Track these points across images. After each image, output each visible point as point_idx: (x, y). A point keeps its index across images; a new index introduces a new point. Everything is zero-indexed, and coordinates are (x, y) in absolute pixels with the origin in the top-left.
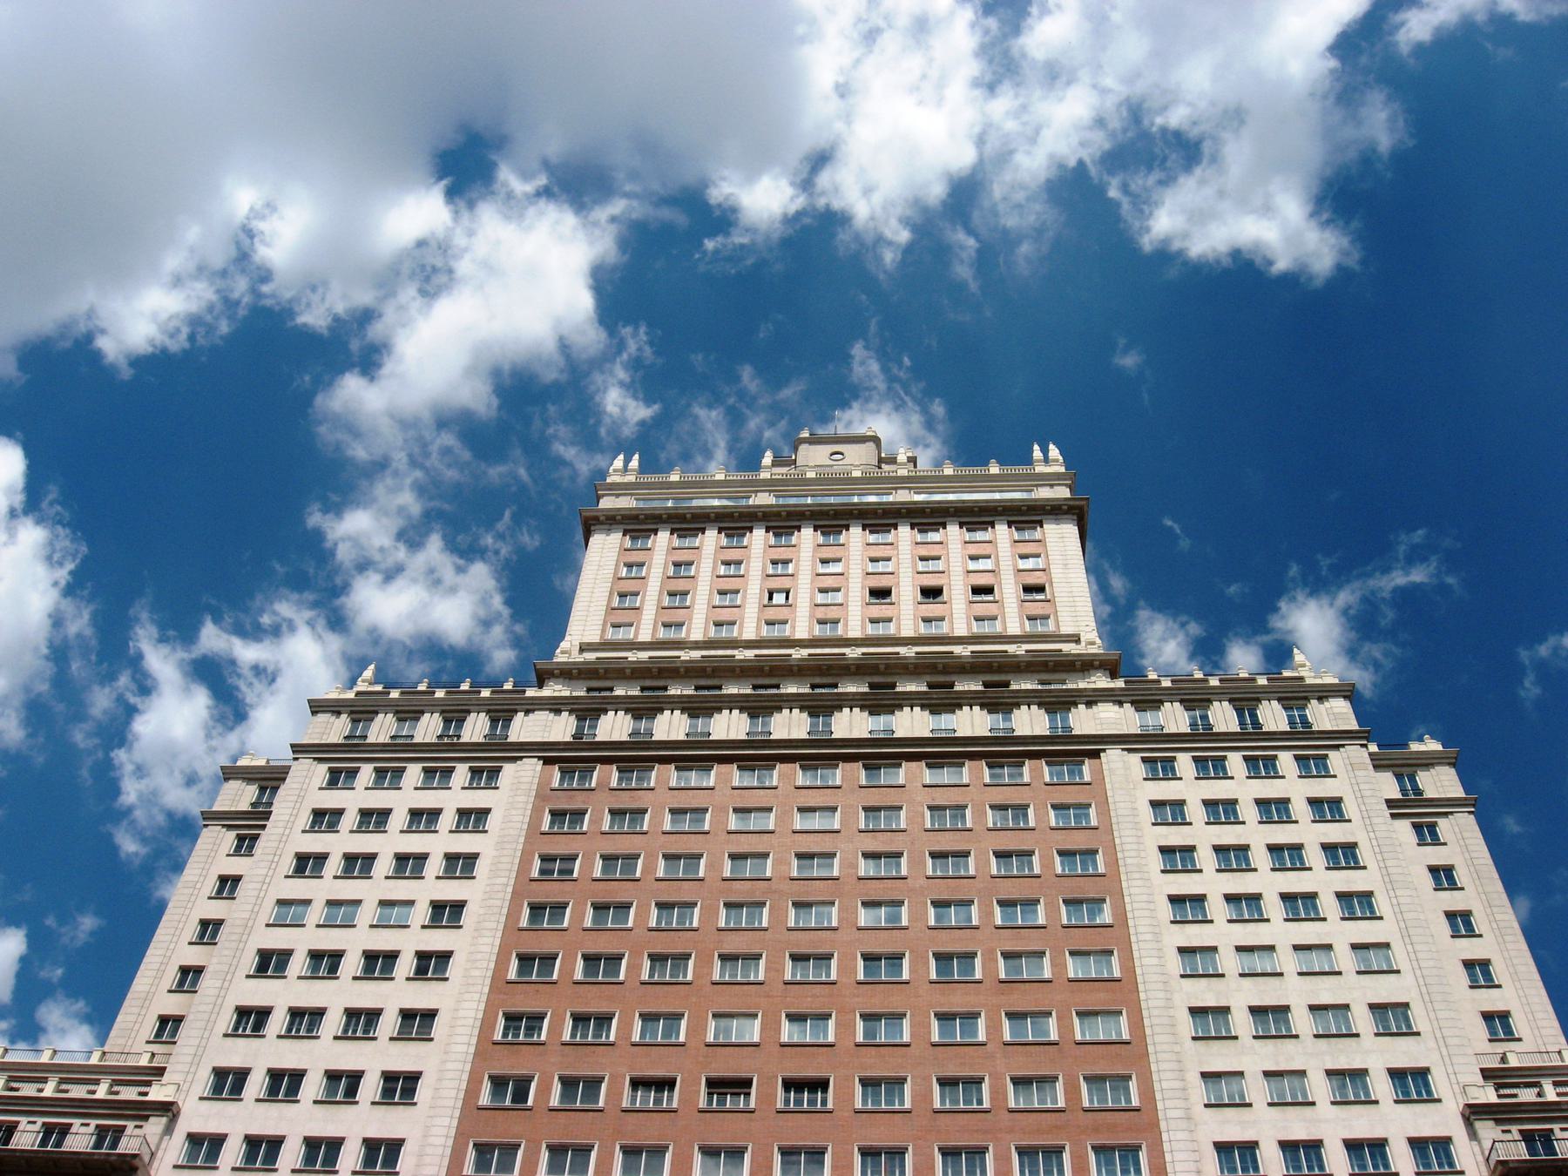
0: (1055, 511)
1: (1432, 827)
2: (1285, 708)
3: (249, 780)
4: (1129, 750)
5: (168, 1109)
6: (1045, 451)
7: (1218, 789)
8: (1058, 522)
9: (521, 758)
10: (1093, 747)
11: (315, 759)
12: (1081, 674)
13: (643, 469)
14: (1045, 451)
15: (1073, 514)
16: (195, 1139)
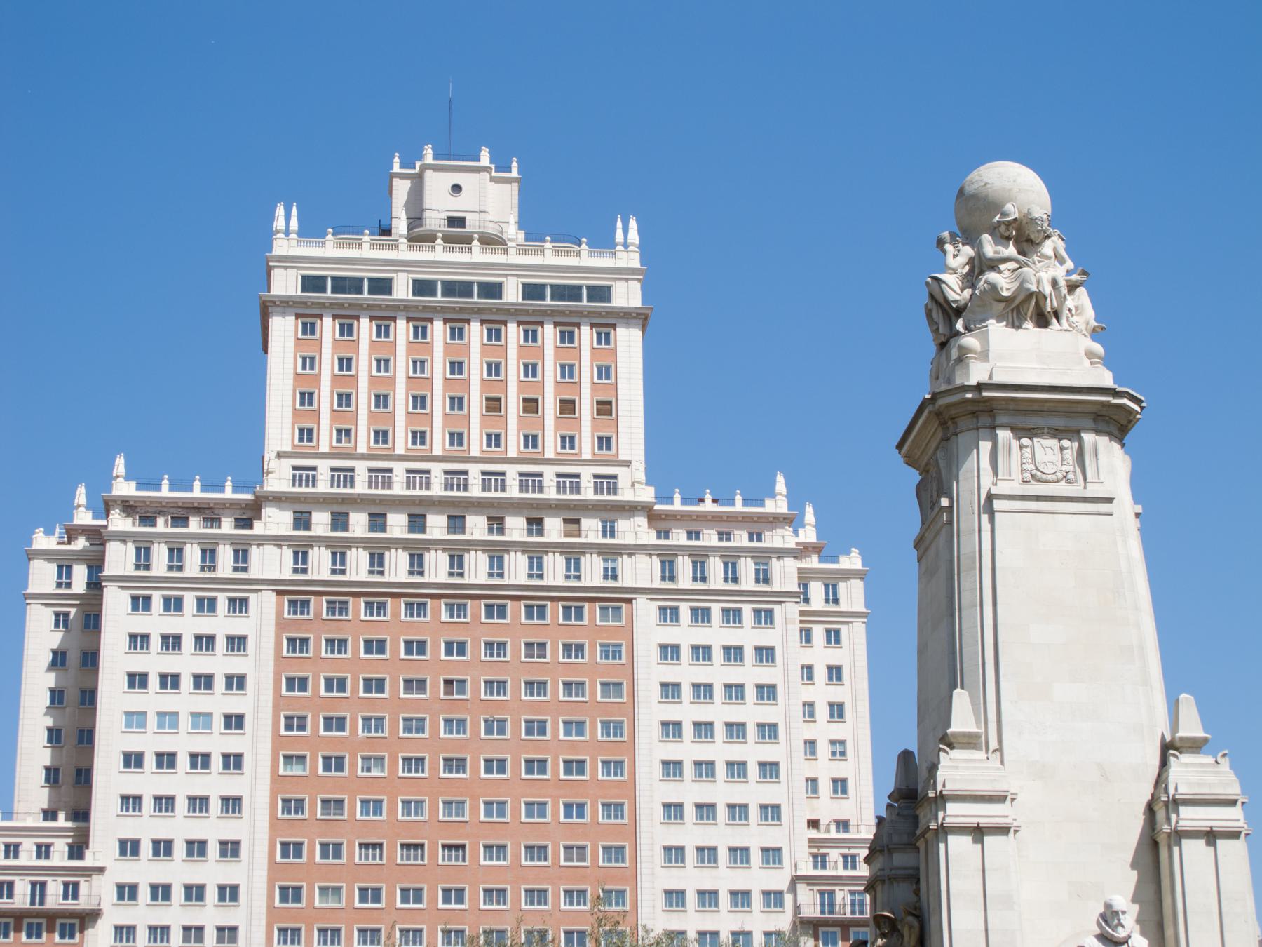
1: (837, 632)
2: (756, 564)
3: (49, 560)
4: (652, 599)
5: (101, 870)
7: (701, 635)
8: (628, 326)
9: (261, 590)
10: (626, 597)
11: (119, 587)
12: (627, 514)
13: (301, 233)
15: (640, 319)
16: (120, 887)
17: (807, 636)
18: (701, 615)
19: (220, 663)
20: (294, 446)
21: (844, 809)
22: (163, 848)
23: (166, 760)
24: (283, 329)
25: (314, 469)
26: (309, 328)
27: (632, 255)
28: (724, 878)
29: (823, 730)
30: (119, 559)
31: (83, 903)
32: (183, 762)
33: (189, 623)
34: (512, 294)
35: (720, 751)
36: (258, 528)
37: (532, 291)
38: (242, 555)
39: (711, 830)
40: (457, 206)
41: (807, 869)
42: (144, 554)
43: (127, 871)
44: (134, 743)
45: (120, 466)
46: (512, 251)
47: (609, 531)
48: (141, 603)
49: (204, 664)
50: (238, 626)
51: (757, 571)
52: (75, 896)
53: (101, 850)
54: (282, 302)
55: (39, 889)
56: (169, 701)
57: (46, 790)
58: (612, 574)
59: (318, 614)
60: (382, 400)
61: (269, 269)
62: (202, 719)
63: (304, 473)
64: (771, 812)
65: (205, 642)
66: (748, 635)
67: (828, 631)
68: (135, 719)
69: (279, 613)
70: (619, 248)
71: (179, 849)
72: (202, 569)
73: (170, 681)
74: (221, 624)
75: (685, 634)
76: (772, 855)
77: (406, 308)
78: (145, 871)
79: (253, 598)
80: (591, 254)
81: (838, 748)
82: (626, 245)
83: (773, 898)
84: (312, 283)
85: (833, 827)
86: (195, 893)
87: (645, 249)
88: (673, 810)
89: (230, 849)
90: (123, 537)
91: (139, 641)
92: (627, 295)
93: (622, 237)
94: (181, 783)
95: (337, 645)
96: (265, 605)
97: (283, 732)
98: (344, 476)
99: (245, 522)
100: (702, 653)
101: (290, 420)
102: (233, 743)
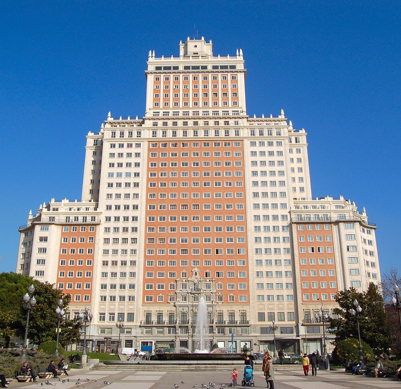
0: (240, 72)
1: (300, 150)
5: (101, 213)
6: (239, 52)
7: (262, 149)
14: (239, 52)
16: (107, 218)
17: (291, 151)
19: (133, 160)
21: (304, 195)
22: (118, 207)
23: (119, 185)
24: (151, 79)
25: (159, 112)
26: (158, 79)
27: (241, 58)
28: (271, 212)
29: (297, 175)
30: (108, 135)
31: (96, 222)
32: (123, 185)
33: (125, 150)
34: (210, 68)
35: (268, 178)
37: (215, 67)
38: (139, 133)
39: (267, 199)
41: (293, 209)
42: (114, 134)
43: (109, 214)
44: (111, 180)
45: (109, 114)
47: (237, 123)
48: (113, 146)
49: (129, 160)
50: (138, 150)
51: (277, 132)
52: (94, 220)
53: (102, 208)
54: (150, 73)
55: (85, 219)
56: (120, 170)
57: (90, 195)
58: (237, 133)
59: (159, 147)
60: (176, 95)
61: (147, 65)
62: (128, 175)
63: (156, 114)
64: (283, 194)
65: (129, 155)
66: (275, 148)
67: (297, 149)
68: (111, 175)
69: (149, 147)
70: (238, 56)
71: (122, 208)
72: (129, 137)
73: (120, 165)
74: (134, 150)
75: (258, 149)
76: (284, 206)
77: (183, 72)
78: (113, 213)
79: (142, 143)
80: (230, 58)
82: (239, 55)
83: (284, 217)
84: (158, 68)
85: (300, 199)
86: (126, 219)
87: (244, 56)
88: (256, 195)
89: (136, 207)
90: (108, 129)
91: (112, 155)
92: (240, 66)
93: (238, 53)
94: (123, 191)
95: (164, 155)
96: (145, 145)
97: (150, 177)
102: (137, 180)
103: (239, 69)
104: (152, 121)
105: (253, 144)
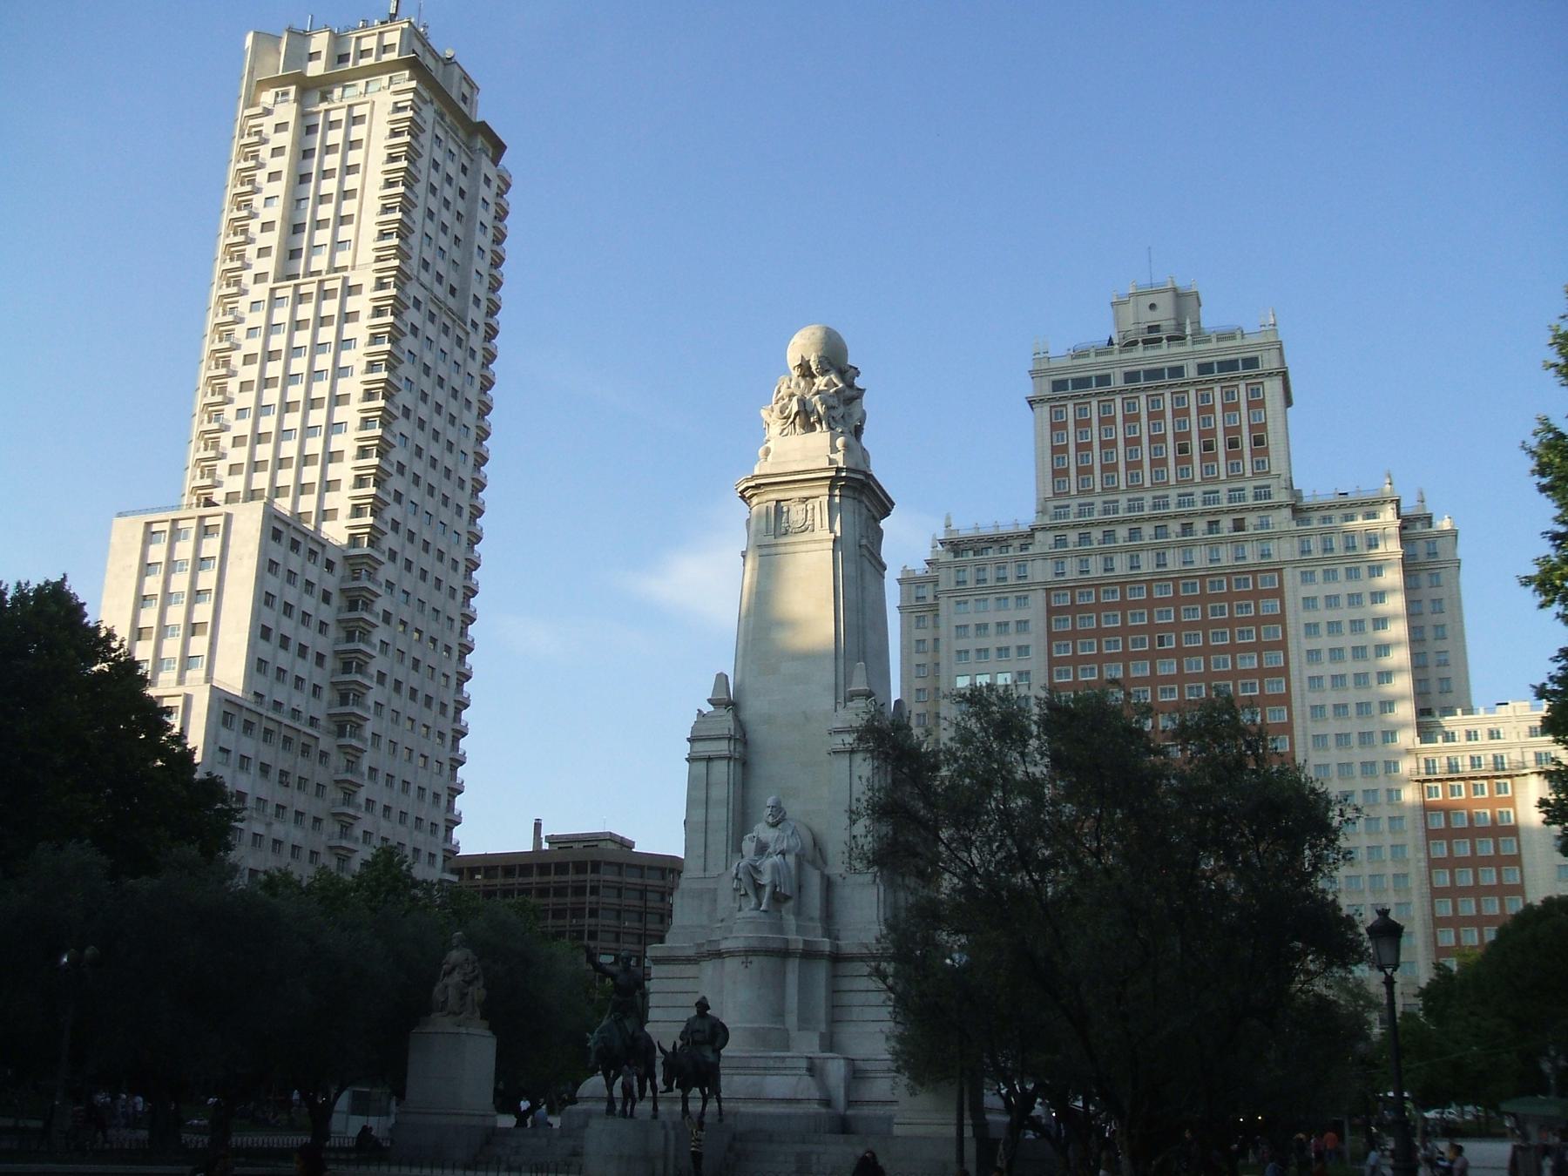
7: (1332, 589)
18: (1330, 575)
19: (1012, 640)
20: (1054, 493)
26: (1059, 414)
36: (1032, 550)
37: (1204, 368)
40: (1151, 318)
46: (1189, 343)
69: (1048, 603)
74: (1012, 614)
75: (1319, 589)
77: (1121, 392)
79: (1032, 595)
81: (1442, 657)
96: (1037, 600)
98: (1086, 509)
99: (1024, 547)
100: (1332, 601)
101: (1050, 476)
103: (1266, 366)
104: (1049, 537)
105: (1307, 577)
